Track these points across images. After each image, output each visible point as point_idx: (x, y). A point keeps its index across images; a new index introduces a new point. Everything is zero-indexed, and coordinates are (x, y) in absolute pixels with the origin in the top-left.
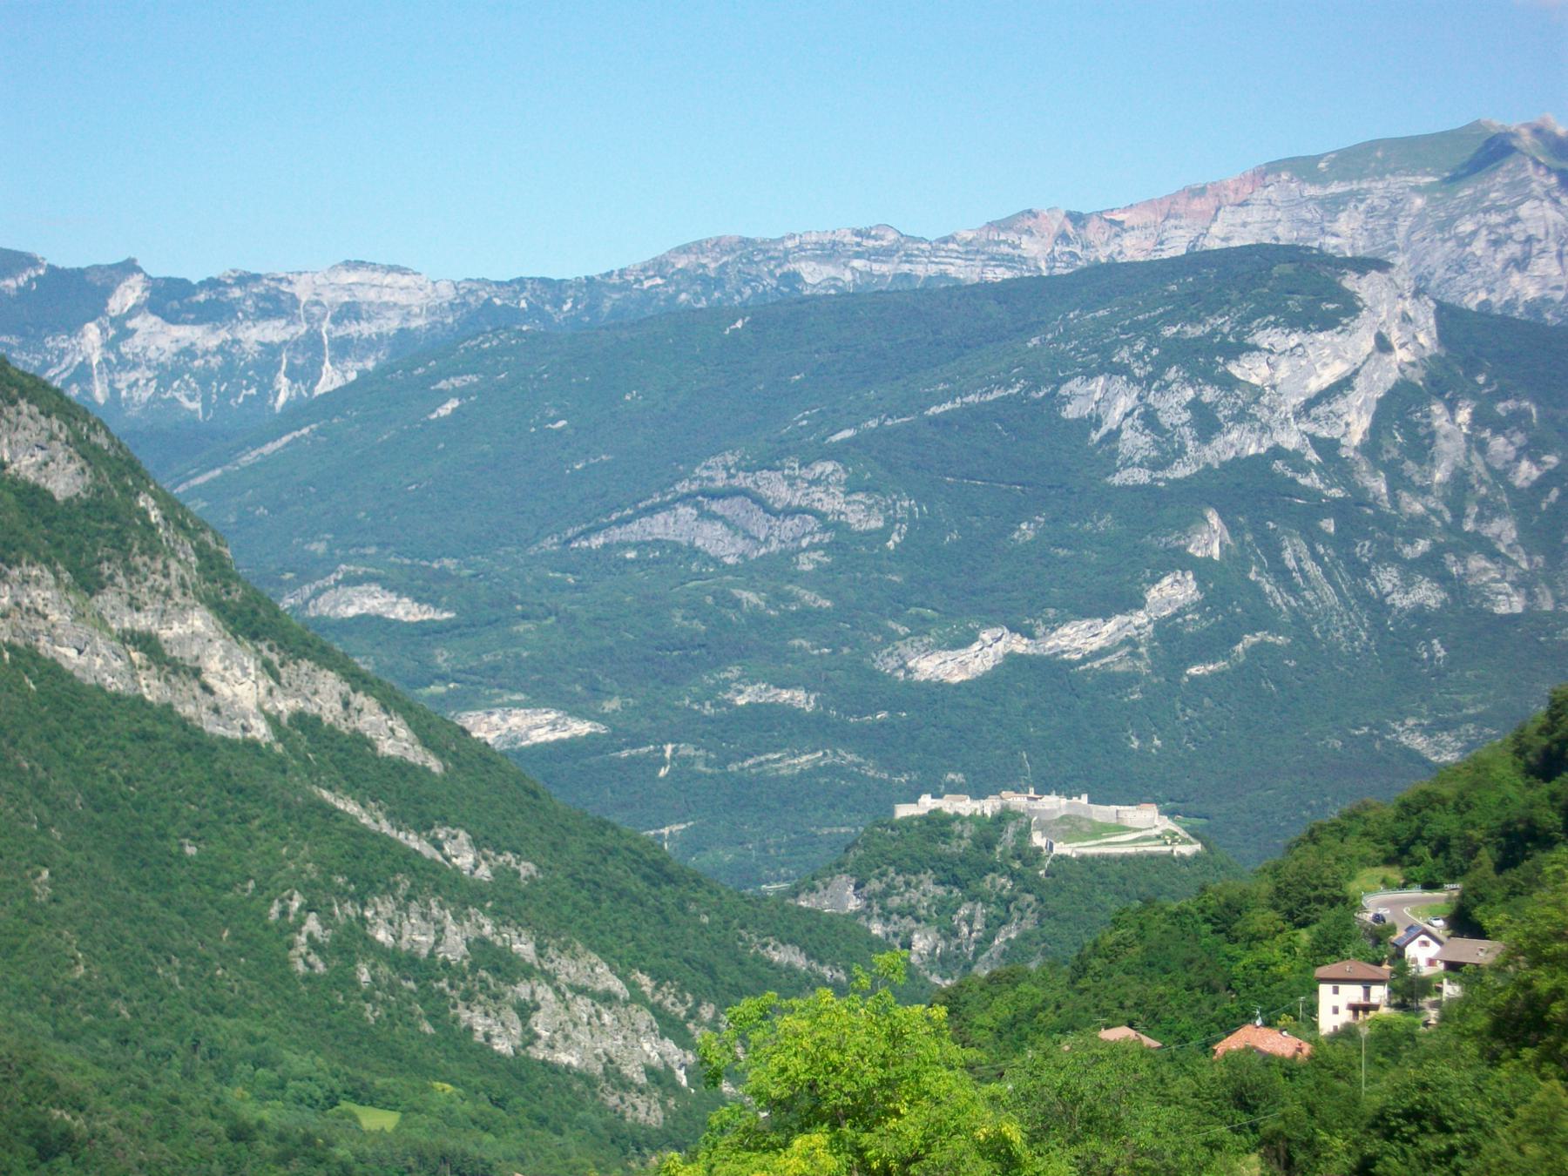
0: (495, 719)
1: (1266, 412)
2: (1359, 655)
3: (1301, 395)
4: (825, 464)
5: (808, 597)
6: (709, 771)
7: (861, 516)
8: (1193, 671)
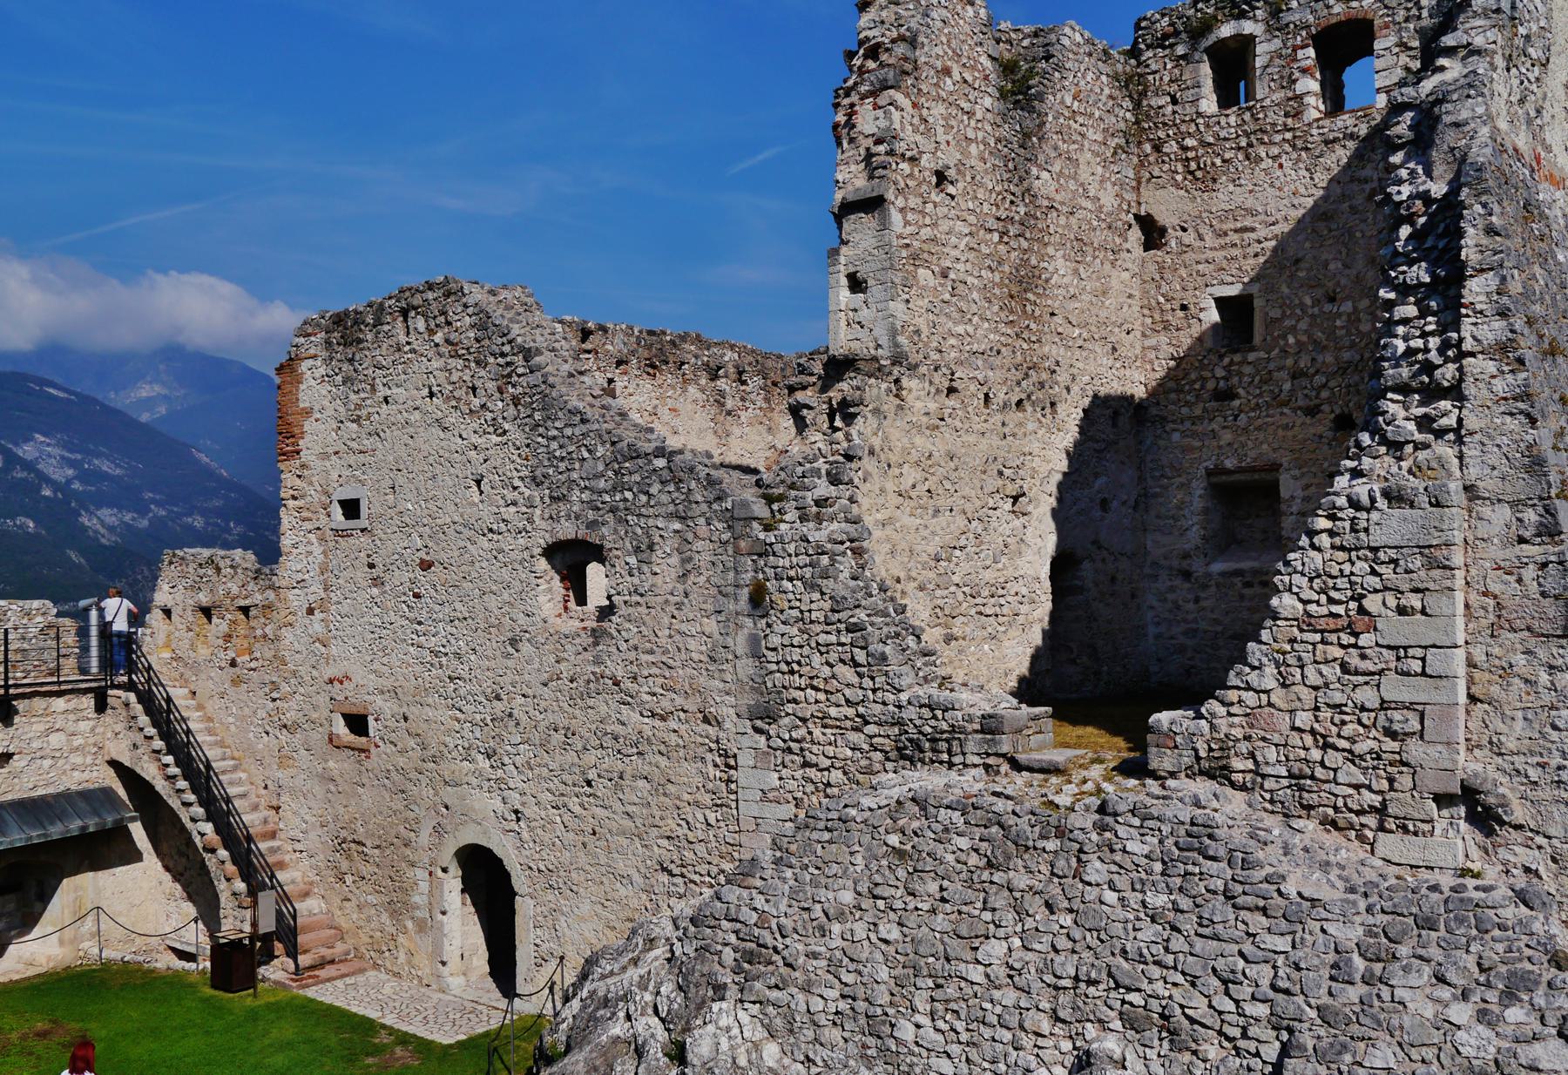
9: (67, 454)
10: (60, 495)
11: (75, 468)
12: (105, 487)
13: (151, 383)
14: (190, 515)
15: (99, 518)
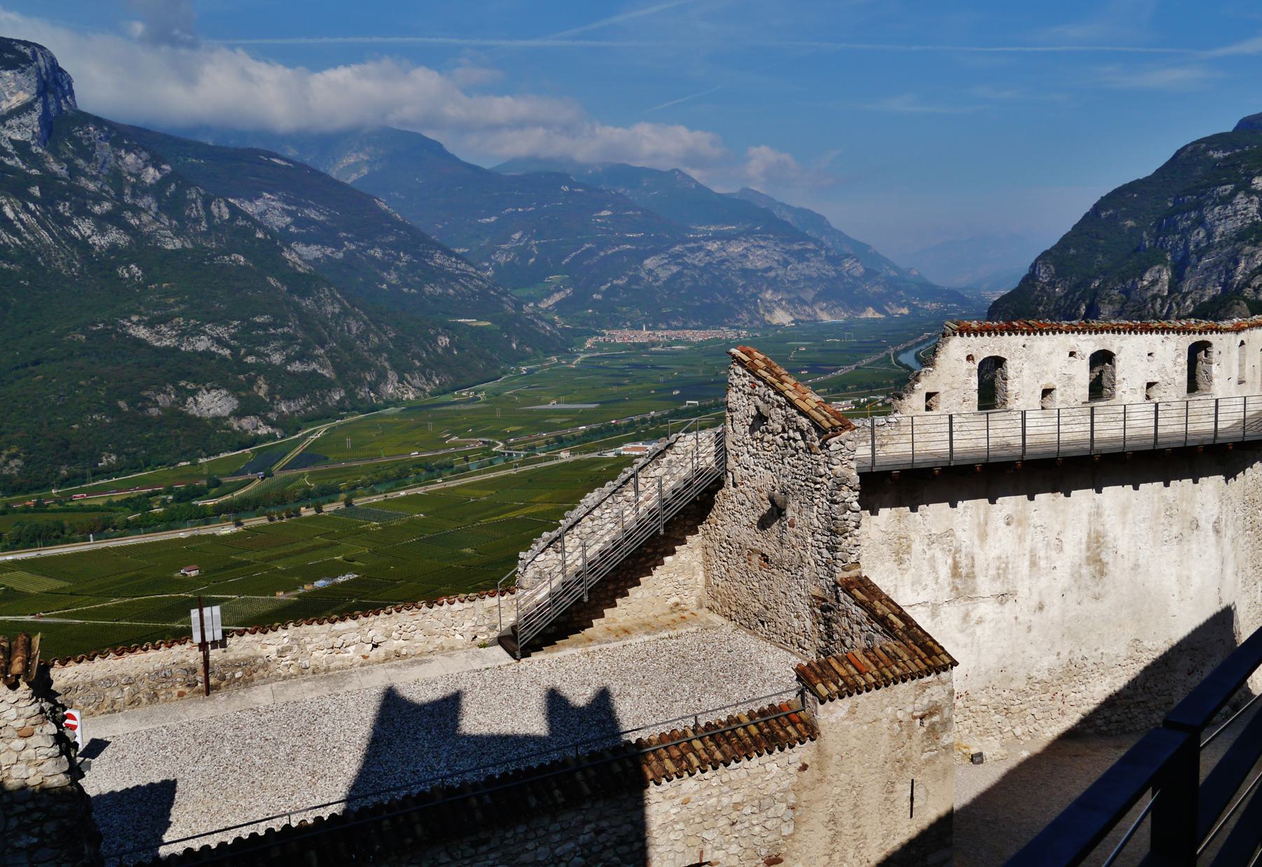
2: (78, 277)
9: (286, 207)
10: (269, 237)
11: (291, 217)
12: (312, 229)
13: (357, 151)
14: (372, 248)
15: (297, 253)
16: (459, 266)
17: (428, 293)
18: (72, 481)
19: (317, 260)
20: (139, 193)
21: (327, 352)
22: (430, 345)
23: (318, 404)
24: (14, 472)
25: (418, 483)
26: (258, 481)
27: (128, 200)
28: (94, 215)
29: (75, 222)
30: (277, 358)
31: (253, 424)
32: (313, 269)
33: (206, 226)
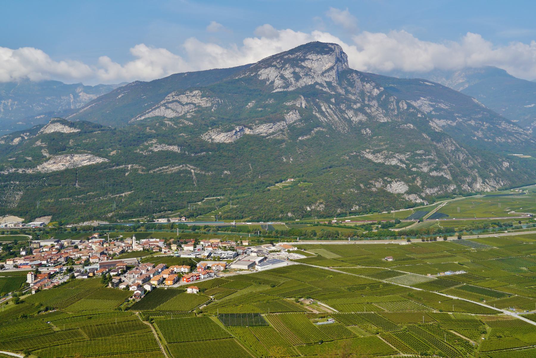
0: (68, 158)
1: (313, 73)
2: (346, 134)
3: (321, 71)
4: (196, 91)
5: (186, 122)
6: (143, 173)
7: (204, 103)
8: (300, 138)
10: (423, 116)
15: (435, 123)
16: (514, 128)
17: (497, 141)
18: (341, 215)
19: (443, 126)
20: (371, 99)
21: (448, 168)
22: (499, 166)
23: (444, 191)
24: (321, 210)
25: (494, 231)
26: (417, 223)
27: (366, 102)
28: (354, 109)
29: (346, 112)
30: (425, 170)
31: (414, 198)
32: (442, 130)
33: (397, 112)
